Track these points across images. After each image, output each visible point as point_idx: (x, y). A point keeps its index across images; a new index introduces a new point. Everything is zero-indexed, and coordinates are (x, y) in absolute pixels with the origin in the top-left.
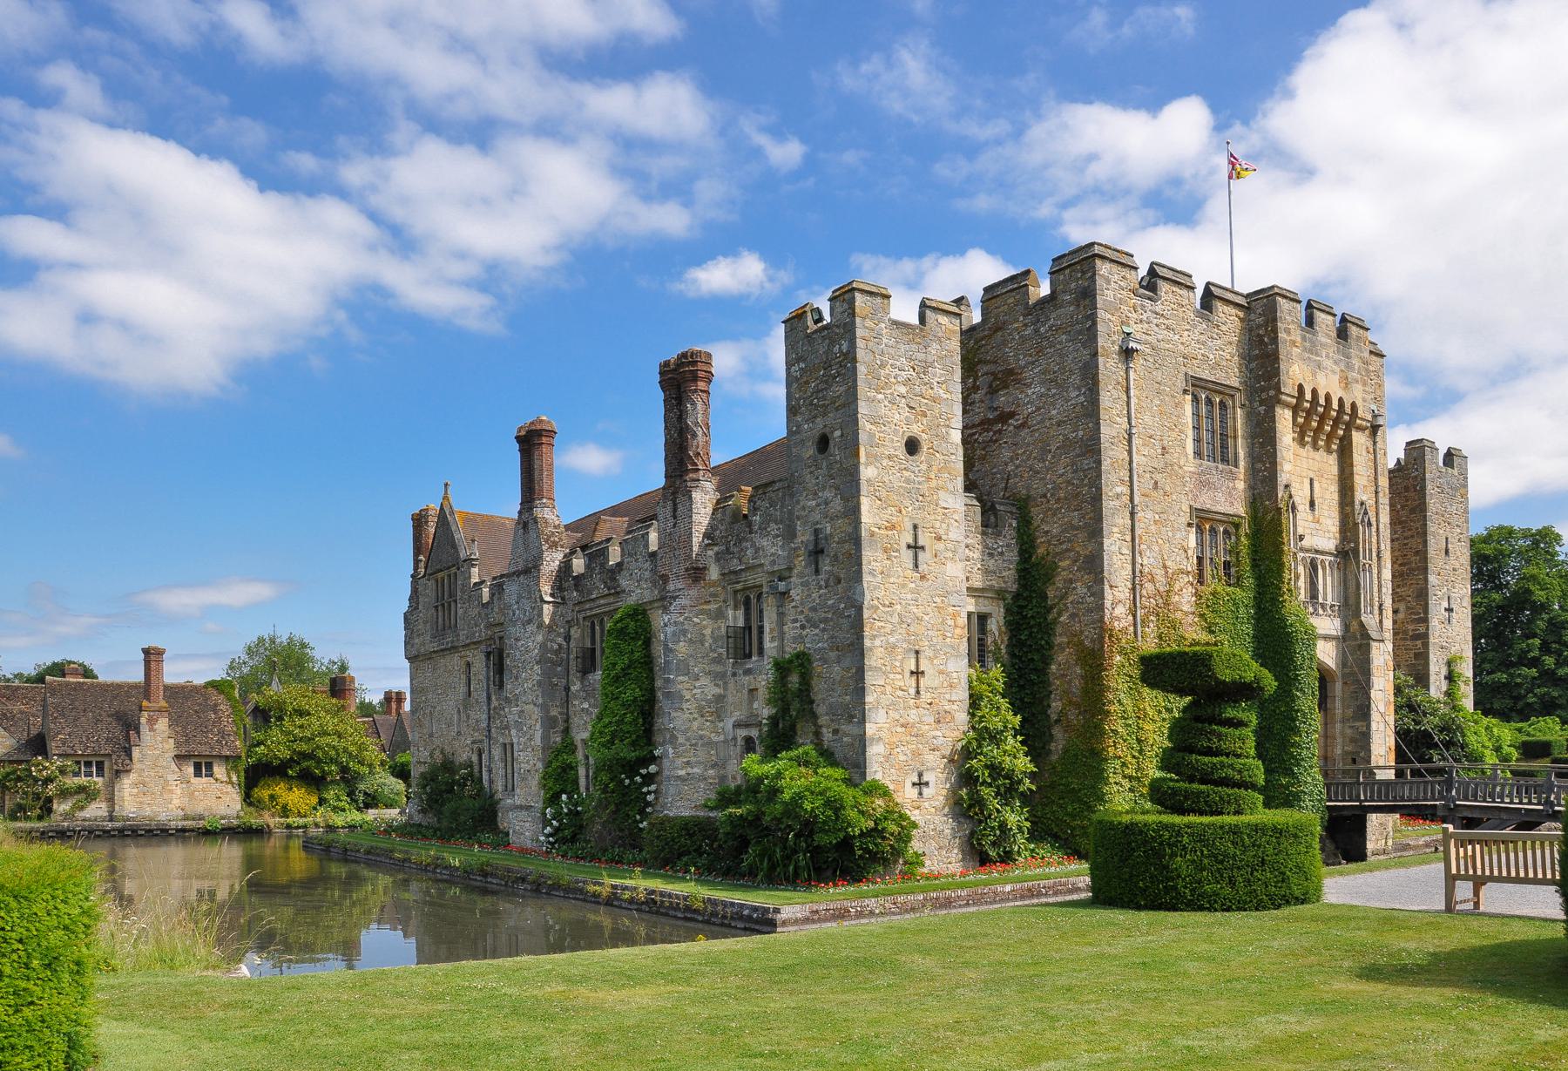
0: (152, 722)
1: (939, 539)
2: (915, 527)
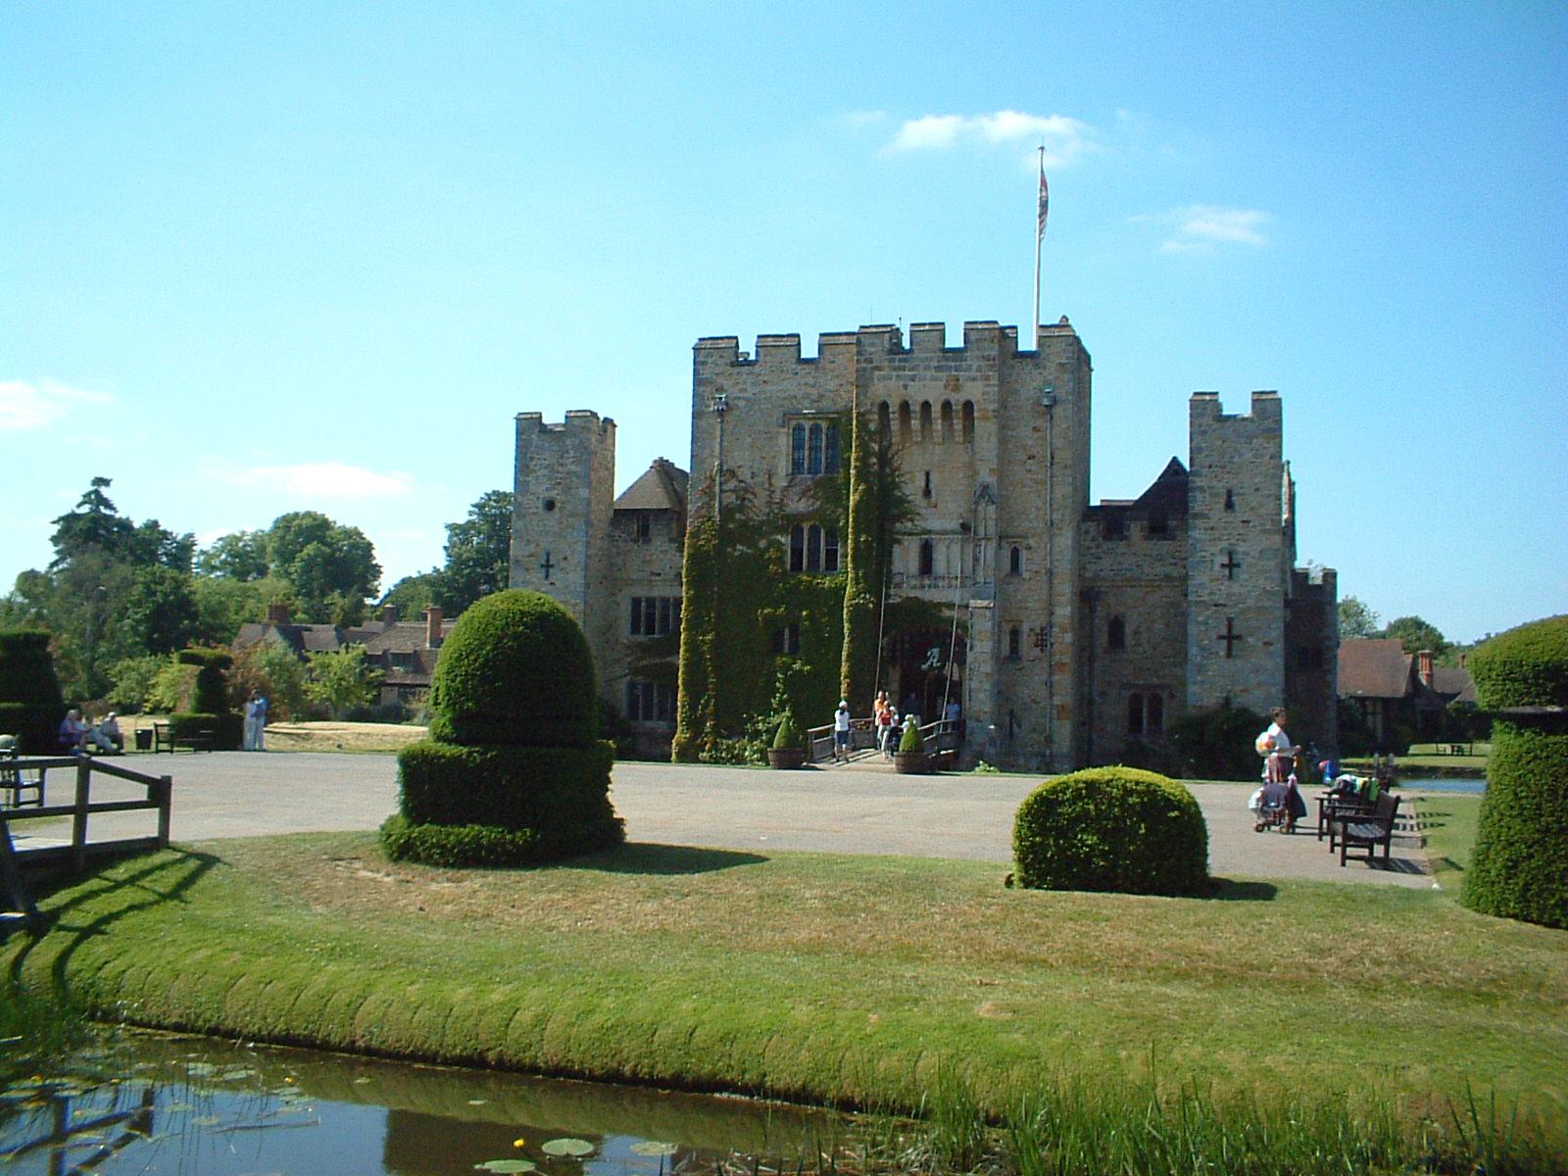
1: (565, 558)
2: (548, 554)
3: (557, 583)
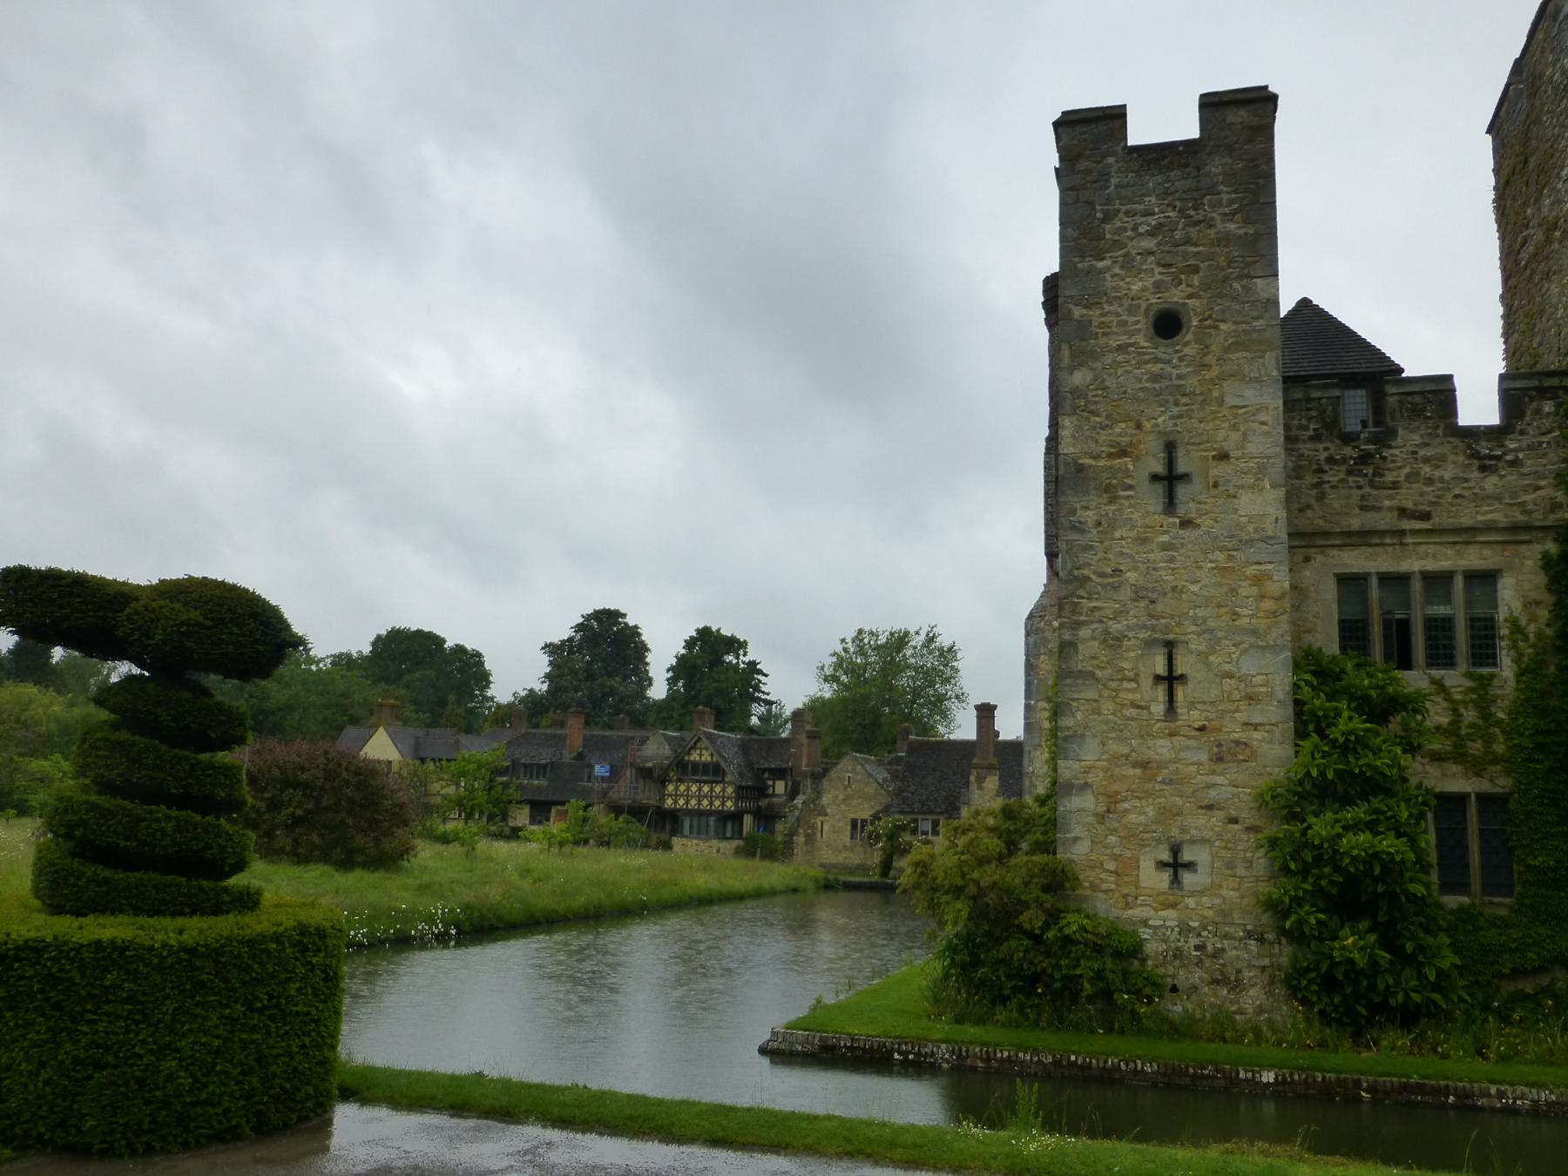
0: (980, 780)
2: (1170, 448)
3: (1205, 522)
